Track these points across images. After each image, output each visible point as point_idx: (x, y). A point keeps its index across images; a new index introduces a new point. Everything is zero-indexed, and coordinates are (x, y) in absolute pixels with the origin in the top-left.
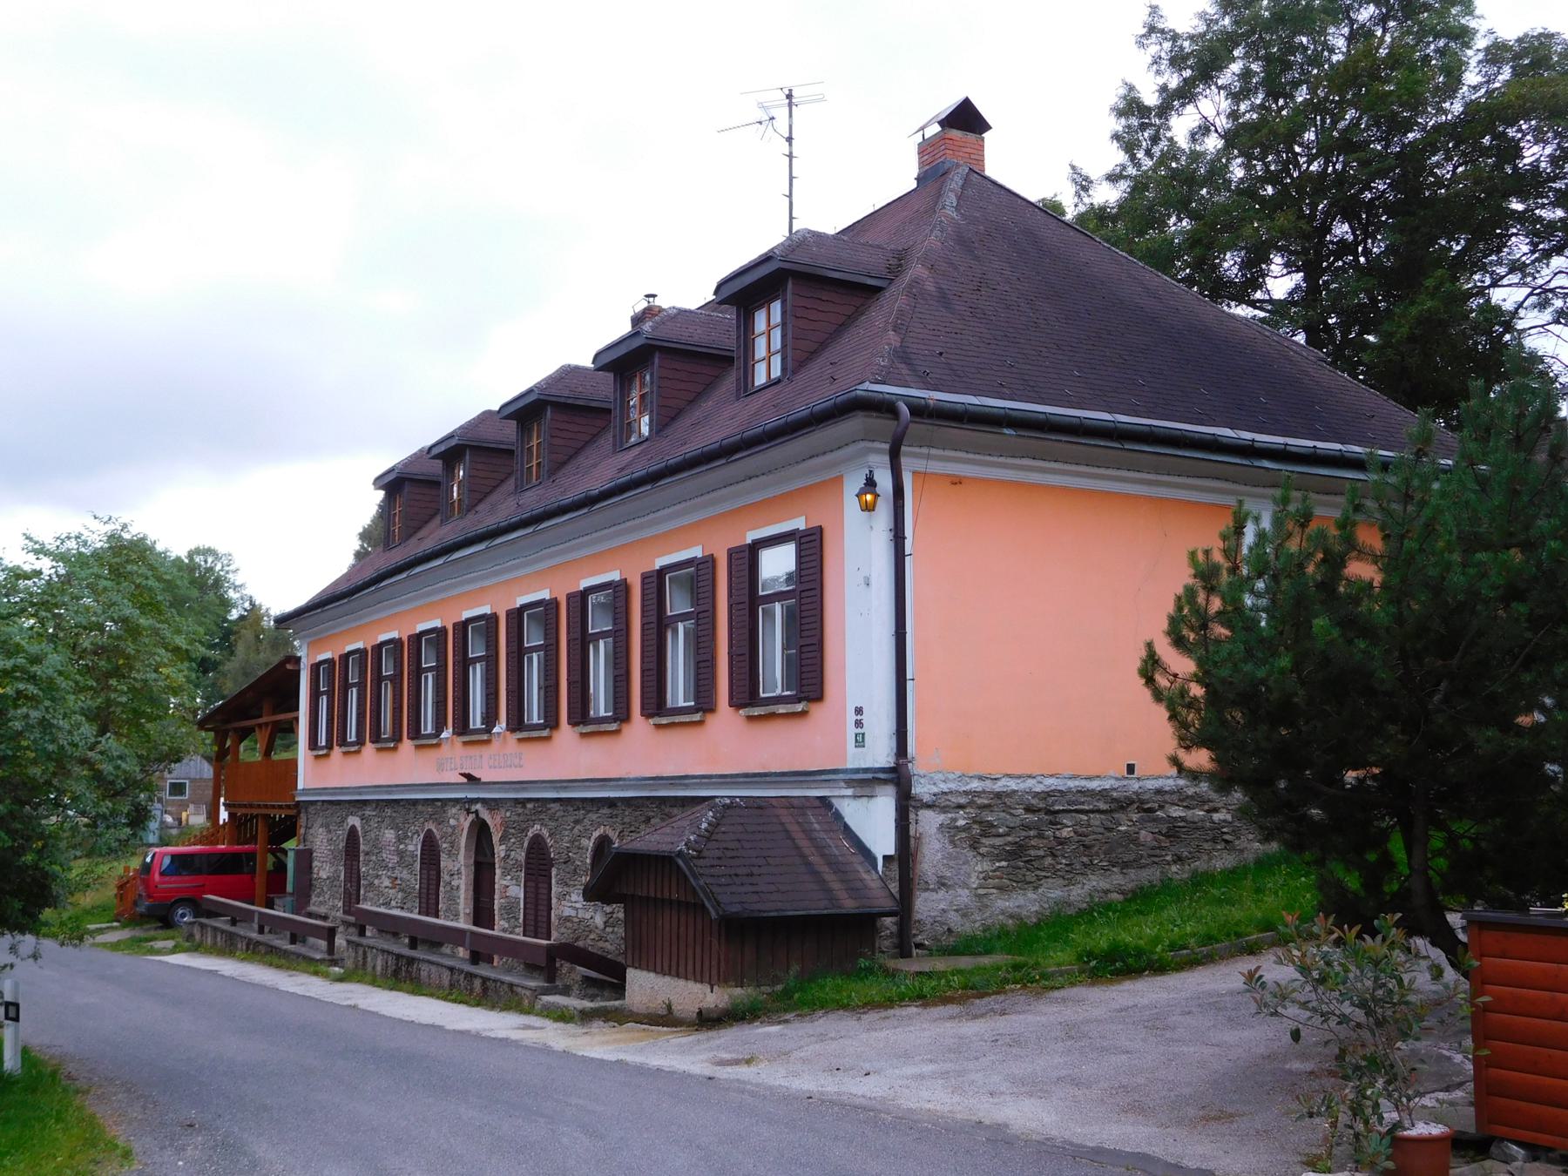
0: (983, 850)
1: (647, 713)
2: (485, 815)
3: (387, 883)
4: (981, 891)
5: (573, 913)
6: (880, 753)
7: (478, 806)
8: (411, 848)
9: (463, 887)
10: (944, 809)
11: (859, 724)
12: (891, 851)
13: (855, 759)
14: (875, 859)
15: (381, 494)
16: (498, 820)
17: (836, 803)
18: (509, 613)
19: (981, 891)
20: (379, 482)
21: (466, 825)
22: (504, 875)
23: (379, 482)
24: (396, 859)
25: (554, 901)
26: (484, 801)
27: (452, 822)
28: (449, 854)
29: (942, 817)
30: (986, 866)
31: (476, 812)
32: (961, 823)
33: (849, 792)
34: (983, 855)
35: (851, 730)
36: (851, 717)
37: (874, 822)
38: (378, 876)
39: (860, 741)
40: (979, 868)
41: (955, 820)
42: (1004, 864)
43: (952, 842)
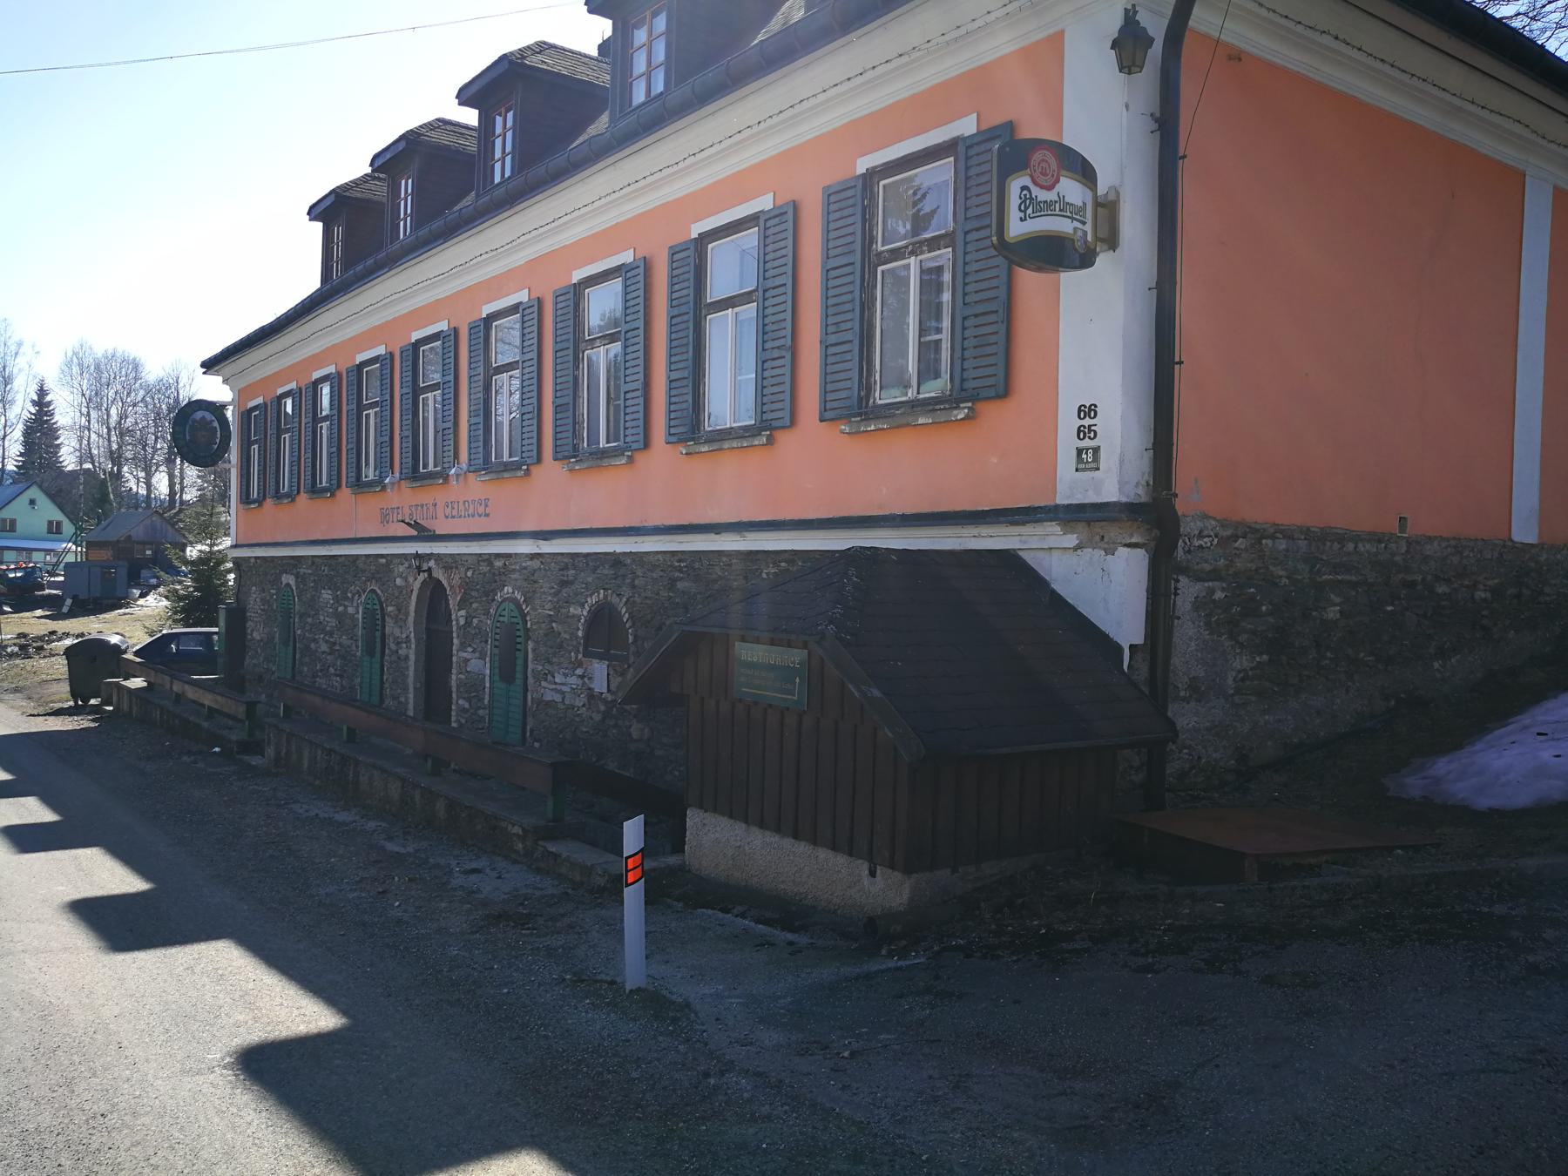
0: (1243, 638)
1: (675, 439)
2: (439, 574)
3: (324, 647)
4: (1237, 699)
5: (558, 698)
6: (1116, 478)
7: (432, 563)
8: (351, 610)
9: (412, 657)
10: (1198, 577)
11: (1081, 432)
12: (1139, 639)
13: (1071, 486)
14: (1120, 649)
15: (319, 226)
16: (456, 581)
17: (1021, 553)
18: (472, 328)
19: (1237, 699)
20: (315, 212)
21: (417, 585)
22: (463, 647)
23: (315, 212)
24: (333, 622)
25: (531, 681)
26: (438, 558)
27: (399, 581)
28: (396, 620)
29: (1198, 586)
30: (1242, 662)
31: (430, 570)
32: (1219, 595)
33: (1071, 540)
34: (1242, 645)
35: (1067, 442)
36: (1068, 422)
37: (1109, 588)
38: (314, 640)
39: (1087, 459)
40: (1237, 665)
41: (1212, 591)
42: (1265, 657)
43: (1208, 624)
